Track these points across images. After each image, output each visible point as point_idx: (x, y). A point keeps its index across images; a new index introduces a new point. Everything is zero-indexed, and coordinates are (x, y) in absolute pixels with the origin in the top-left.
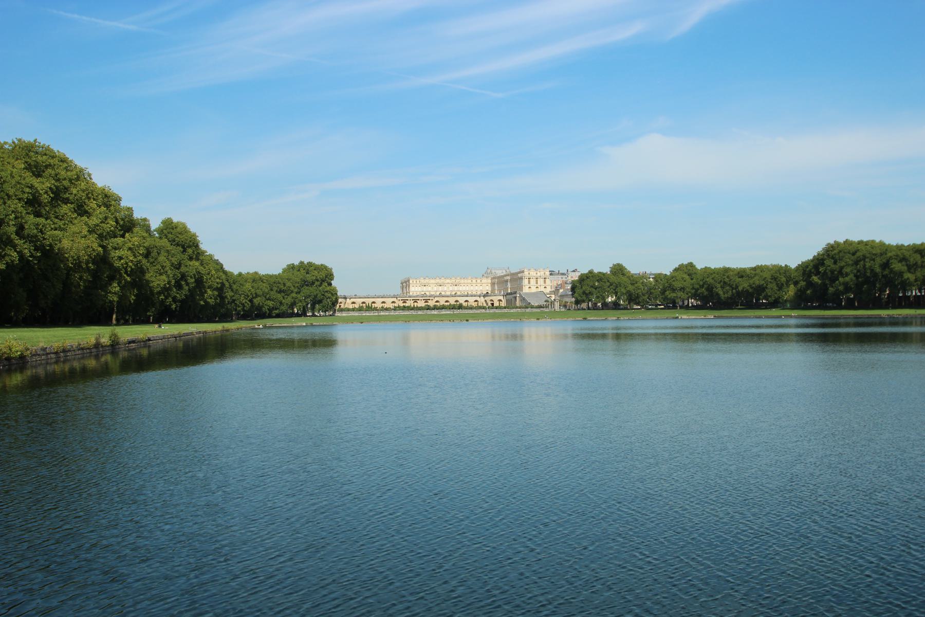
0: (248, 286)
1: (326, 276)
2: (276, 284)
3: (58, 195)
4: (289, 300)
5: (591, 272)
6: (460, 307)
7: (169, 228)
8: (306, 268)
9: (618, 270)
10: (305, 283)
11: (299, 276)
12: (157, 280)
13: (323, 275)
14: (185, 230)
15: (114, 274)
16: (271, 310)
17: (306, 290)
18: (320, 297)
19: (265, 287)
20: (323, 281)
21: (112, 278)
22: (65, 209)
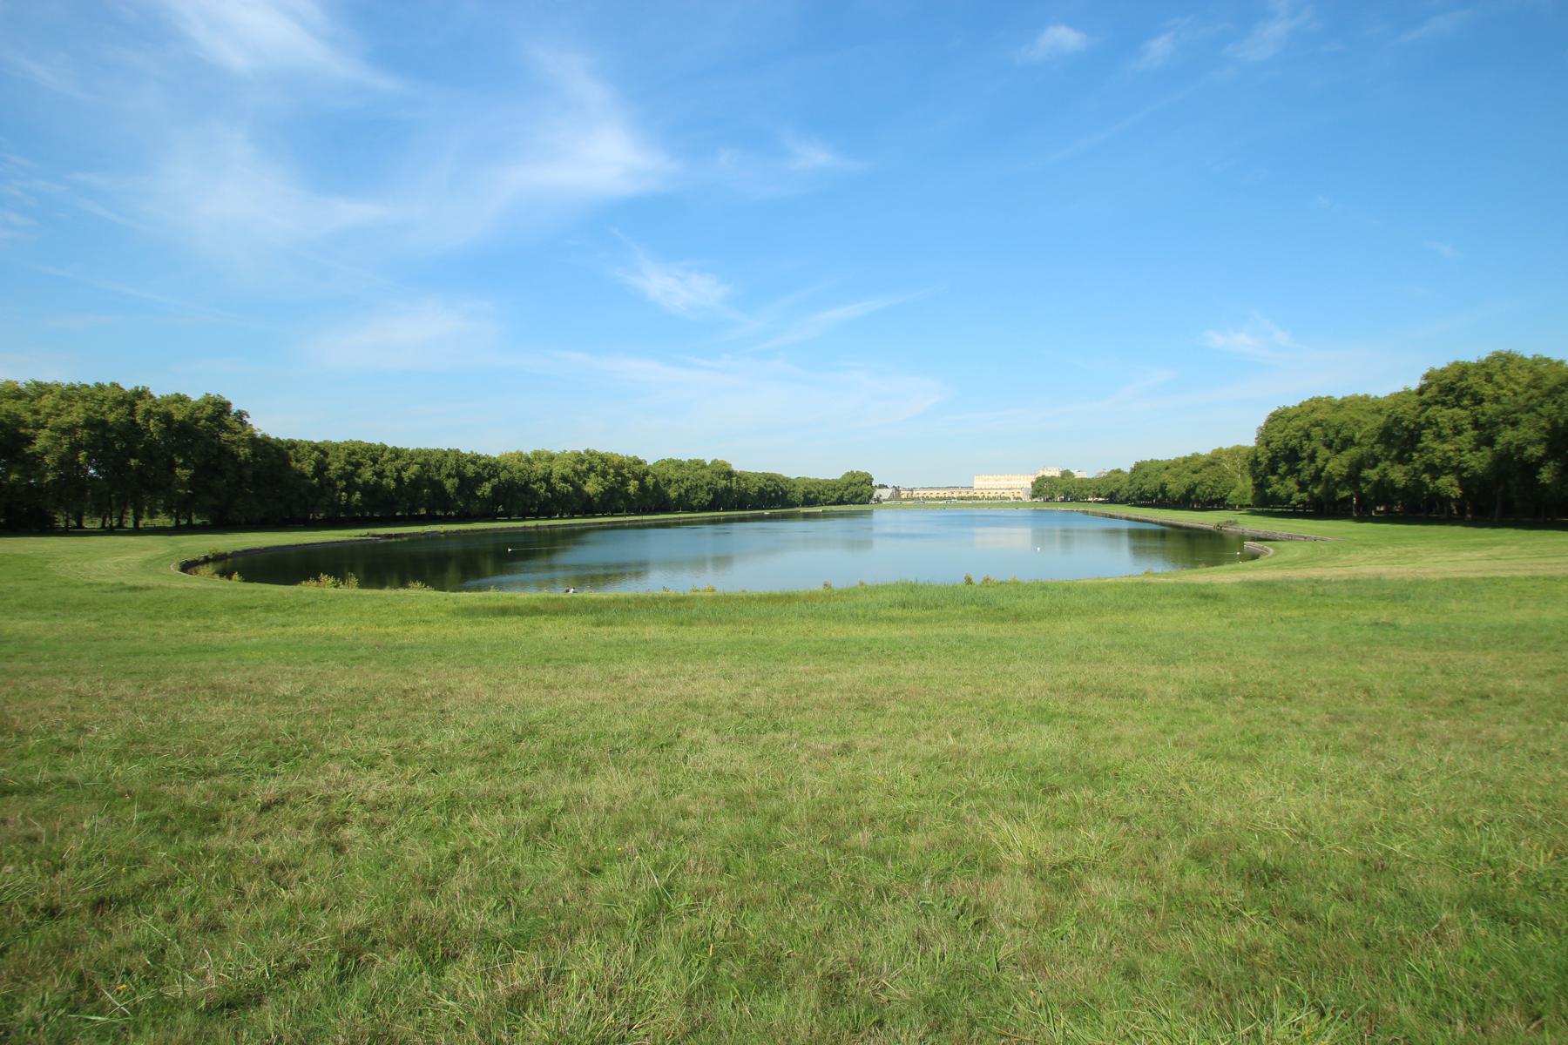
0: (802, 488)
1: (868, 480)
2: (832, 486)
3: (591, 469)
4: (836, 495)
5: (1066, 474)
6: (976, 498)
7: (715, 462)
8: (852, 474)
9: (1066, 474)
10: (851, 484)
11: (849, 478)
12: (673, 493)
13: (862, 479)
14: (725, 464)
15: (627, 496)
16: (825, 500)
17: (850, 489)
18: (859, 493)
19: (821, 488)
20: (864, 482)
21: (621, 498)
22: (592, 475)
